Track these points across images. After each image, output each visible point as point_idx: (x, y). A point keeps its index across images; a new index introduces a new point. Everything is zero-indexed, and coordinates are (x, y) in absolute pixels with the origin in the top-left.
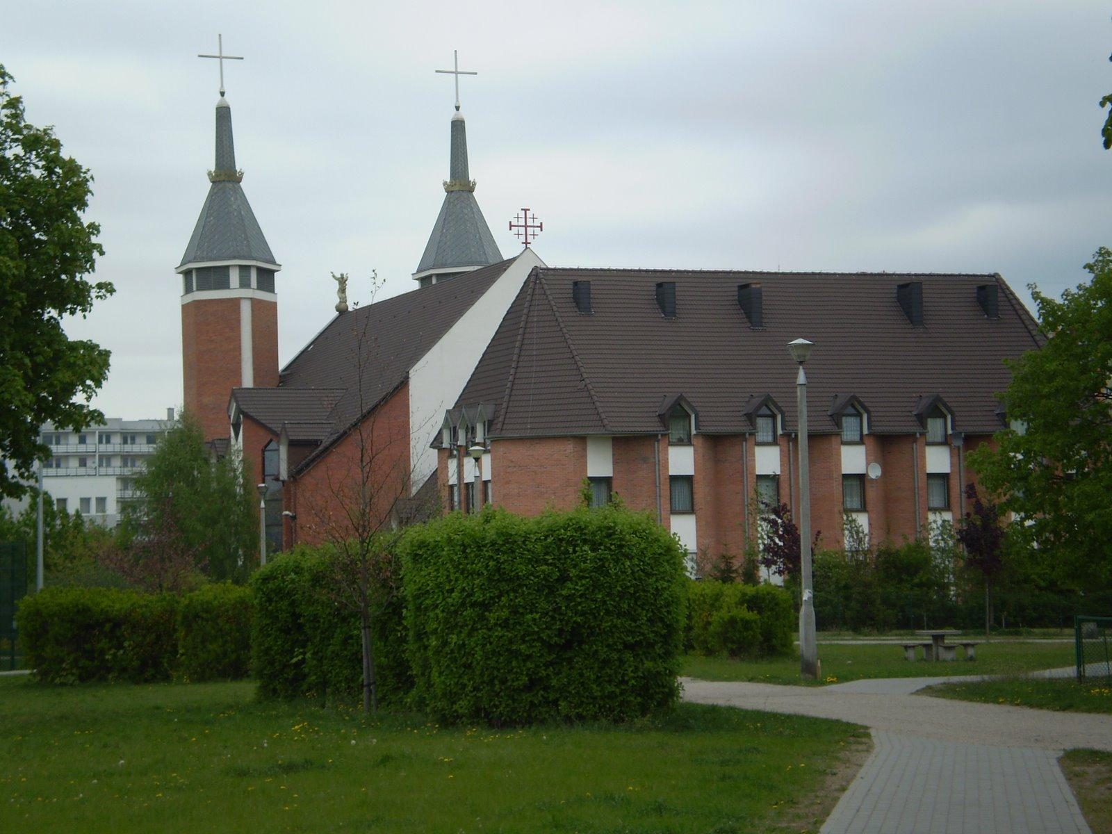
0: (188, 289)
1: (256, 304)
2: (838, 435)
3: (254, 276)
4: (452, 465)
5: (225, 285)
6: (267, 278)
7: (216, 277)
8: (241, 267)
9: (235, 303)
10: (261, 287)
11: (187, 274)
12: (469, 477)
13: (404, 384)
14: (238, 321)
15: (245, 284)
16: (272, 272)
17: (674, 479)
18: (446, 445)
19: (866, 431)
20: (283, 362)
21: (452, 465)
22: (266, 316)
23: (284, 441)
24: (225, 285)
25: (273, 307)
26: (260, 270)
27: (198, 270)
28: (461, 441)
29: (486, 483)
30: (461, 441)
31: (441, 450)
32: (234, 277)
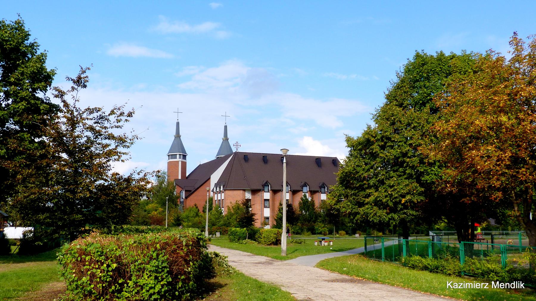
0: (169, 159)
1: (182, 162)
2: (302, 191)
3: (182, 156)
4: (216, 195)
5: (176, 158)
6: (184, 157)
7: (174, 156)
8: (179, 154)
9: (178, 162)
10: (183, 159)
11: (169, 156)
12: (219, 198)
13: (209, 179)
14: (178, 166)
15: (180, 158)
16: (186, 156)
17: (265, 200)
18: (215, 191)
19: (308, 190)
20: (187, 175)
21: (216, 195)
22: (184, 165)
23: (184, 190)
24: (176, 158)
25: (186, 163)
26: (183, 155)
27: (171, 155)
28: (218, 190)
29: (223, 200)
30: (218, 190)
31: (214, 192)
32: (178, 156)
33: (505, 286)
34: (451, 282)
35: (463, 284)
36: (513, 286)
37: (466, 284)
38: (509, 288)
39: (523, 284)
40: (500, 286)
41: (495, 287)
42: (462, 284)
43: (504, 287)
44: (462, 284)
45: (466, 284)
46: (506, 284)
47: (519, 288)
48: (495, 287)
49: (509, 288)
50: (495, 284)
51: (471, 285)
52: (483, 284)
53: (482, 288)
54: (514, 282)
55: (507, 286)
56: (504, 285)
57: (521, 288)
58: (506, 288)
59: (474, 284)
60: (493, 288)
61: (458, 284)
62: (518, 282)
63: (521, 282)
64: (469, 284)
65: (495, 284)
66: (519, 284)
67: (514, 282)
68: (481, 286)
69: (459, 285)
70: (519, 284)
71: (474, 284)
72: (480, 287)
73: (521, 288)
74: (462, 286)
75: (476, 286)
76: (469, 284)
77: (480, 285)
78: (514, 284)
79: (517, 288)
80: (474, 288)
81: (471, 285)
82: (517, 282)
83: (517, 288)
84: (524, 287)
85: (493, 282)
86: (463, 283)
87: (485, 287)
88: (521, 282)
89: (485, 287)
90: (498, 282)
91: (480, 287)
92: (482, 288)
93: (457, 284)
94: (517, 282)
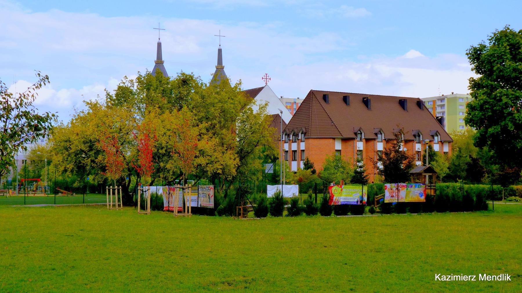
33: (492, 278)
34: (440, 274)
35: (451, 277)
36: (499, 277)
37: (454, 276)
38: (496, 280)
39: (510, 276)
40: (487, 278)
41: (482, 280)
42: (450, 276)
43: (491, 279)
44: (450, 276)
45: (454, 276)
46: (493, 276)
47: (505, 280)
48: (482, 280)
49: (496, 280)
50: (483, 275)
51: (458, 277)
52: (471, 276)
53: (469, 280)
54: (501, 274)
55: (494, 277)
56: (491, 278)
57: (507, 280)
58: (493, 280)
59: (462, 276)
60: (480, 280)
61: (446, 277)
62: (504, 275)
63: (507, 274)
64: (457, 277)
65: (483, 275)
66: (505, 276)
67: (501, 274)
68: (468, 279)
69: (447, 278)
70: (505, 276)
71: (462, 276)
72: (467, 279)
73: (507, 280)
74: (450, 278)
75: (464, 278)
76: (457, 277)
77: (467, 278)
78: (501, 276)
79: (503, 280)
80: (462, 280)
81: (458, 277)
82: (503, 274)
83: (503, 280)
84: (510, 280)
85: (480, 275)
86: (451, 275)
87: (472, 280)
88: (507, 274)
89: (472, 280)
90: (485, 275)
91: (467, 279)
92: (469, 280)
93: (445, 276)
94: (503, 274)
